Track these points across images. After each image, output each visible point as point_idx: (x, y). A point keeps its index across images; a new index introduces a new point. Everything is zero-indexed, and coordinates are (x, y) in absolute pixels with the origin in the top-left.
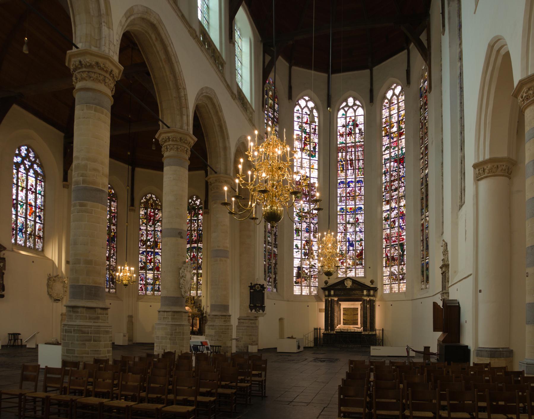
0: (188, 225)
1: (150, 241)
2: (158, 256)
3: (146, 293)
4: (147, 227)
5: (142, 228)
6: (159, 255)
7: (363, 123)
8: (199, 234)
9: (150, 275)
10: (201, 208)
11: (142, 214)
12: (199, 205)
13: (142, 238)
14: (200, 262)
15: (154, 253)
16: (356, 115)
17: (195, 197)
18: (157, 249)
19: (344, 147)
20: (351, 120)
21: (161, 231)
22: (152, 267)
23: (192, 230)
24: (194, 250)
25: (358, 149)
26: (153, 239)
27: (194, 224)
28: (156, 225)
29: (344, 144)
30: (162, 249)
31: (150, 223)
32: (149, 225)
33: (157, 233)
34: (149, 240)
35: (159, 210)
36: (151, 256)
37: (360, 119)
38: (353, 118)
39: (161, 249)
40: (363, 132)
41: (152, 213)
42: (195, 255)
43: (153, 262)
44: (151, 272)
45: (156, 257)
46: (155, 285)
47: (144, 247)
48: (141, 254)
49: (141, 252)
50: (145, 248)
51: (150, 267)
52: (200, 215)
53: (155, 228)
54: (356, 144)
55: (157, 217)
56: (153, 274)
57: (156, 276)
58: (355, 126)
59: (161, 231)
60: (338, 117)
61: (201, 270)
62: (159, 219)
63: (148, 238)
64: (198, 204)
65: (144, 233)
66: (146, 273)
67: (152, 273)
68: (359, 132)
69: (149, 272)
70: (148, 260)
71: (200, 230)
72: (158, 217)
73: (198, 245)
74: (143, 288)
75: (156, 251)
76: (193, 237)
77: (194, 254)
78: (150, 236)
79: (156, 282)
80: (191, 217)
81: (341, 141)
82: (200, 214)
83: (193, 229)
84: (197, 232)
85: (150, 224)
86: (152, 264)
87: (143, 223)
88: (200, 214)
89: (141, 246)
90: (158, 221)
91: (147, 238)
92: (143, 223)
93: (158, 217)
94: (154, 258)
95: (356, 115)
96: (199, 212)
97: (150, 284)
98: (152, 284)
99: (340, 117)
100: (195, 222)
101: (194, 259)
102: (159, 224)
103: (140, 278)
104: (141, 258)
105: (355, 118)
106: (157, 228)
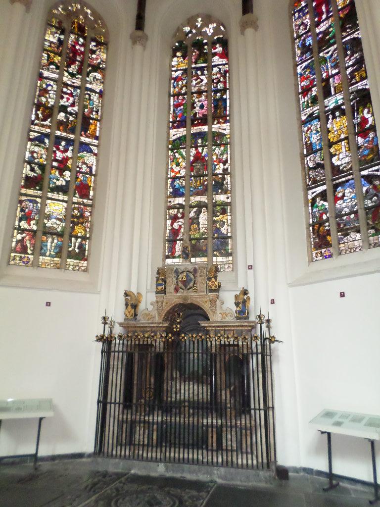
0: (180, 83)
1: (66, 112)
2: (88, 155)
3: (36, 260)
4: (61, 75)
5: (46, 74)
6: (91, 151)
8: (216, 101)
9: (56, 207)
10: (219, 41)
11: (51, 42)
12: (213, 35)
13: (43, 99)
14: (217, 172)
15: (77, 144)
17: (200, 20)
18: (87, 137)
21: (101, 94)
22: (67, 182)
23: (193, 93)
24: (200, 141)
26: (76, 108)
27: (198, 78)
28: (88, 76)
30: (102, 139)
31: (73, 66)
32: (67, 71)
33: (90, 95)
34: (63, 109)
35: (99, 44)
36: (66, 151)
39: (97, 138)
41: (81, 46)
42: (203, 154)
43: (70, 171)
44: (61, 197)
45: (82, 157)
46: (71, 236)
47: (47, 123)
48: (31, 140)
49: (33, 135)
50: (49, 127)
51: (58, 183)
52: (217, 57)
53: (84, 81)
55: (92, 59)
56: (65, 205)
57: (76, 212)
59: (101, 94)
61: (221, 193)
62: (99, 64)
63: (63, 102)
64: (210, 34)
65: (49, 88)
66: (44, 198)
67: (63, 201)
69: (55, 196)
70: (56, 160)
71: (217, 91)
72: (97, 59)
73: (210, 128)
74: (28, 245)
75: (84, 139)
76: (197, 110)
77: (198, 153)
78: (68, 99)
79: (73, 228)
80: (190, 63)
82: (215, 54)
83: (194, 89)
84: (207, 97)
85: (70, 70)
86: (67, 173)
87: (53, 63)
88: (215, 54)
89: (37, 117)
90: (96, 68)
91: (57, 102)
92: (53, 63)
93: (97, 59)
94: (75, 158)
96: (213, 51)
97: (52, 234)
98: (60, 235)
100: (203, 74)
101: (198, 165)
102: (99, 76)
103: (22, 210)
104: (32, 152)
106: (91, 83)
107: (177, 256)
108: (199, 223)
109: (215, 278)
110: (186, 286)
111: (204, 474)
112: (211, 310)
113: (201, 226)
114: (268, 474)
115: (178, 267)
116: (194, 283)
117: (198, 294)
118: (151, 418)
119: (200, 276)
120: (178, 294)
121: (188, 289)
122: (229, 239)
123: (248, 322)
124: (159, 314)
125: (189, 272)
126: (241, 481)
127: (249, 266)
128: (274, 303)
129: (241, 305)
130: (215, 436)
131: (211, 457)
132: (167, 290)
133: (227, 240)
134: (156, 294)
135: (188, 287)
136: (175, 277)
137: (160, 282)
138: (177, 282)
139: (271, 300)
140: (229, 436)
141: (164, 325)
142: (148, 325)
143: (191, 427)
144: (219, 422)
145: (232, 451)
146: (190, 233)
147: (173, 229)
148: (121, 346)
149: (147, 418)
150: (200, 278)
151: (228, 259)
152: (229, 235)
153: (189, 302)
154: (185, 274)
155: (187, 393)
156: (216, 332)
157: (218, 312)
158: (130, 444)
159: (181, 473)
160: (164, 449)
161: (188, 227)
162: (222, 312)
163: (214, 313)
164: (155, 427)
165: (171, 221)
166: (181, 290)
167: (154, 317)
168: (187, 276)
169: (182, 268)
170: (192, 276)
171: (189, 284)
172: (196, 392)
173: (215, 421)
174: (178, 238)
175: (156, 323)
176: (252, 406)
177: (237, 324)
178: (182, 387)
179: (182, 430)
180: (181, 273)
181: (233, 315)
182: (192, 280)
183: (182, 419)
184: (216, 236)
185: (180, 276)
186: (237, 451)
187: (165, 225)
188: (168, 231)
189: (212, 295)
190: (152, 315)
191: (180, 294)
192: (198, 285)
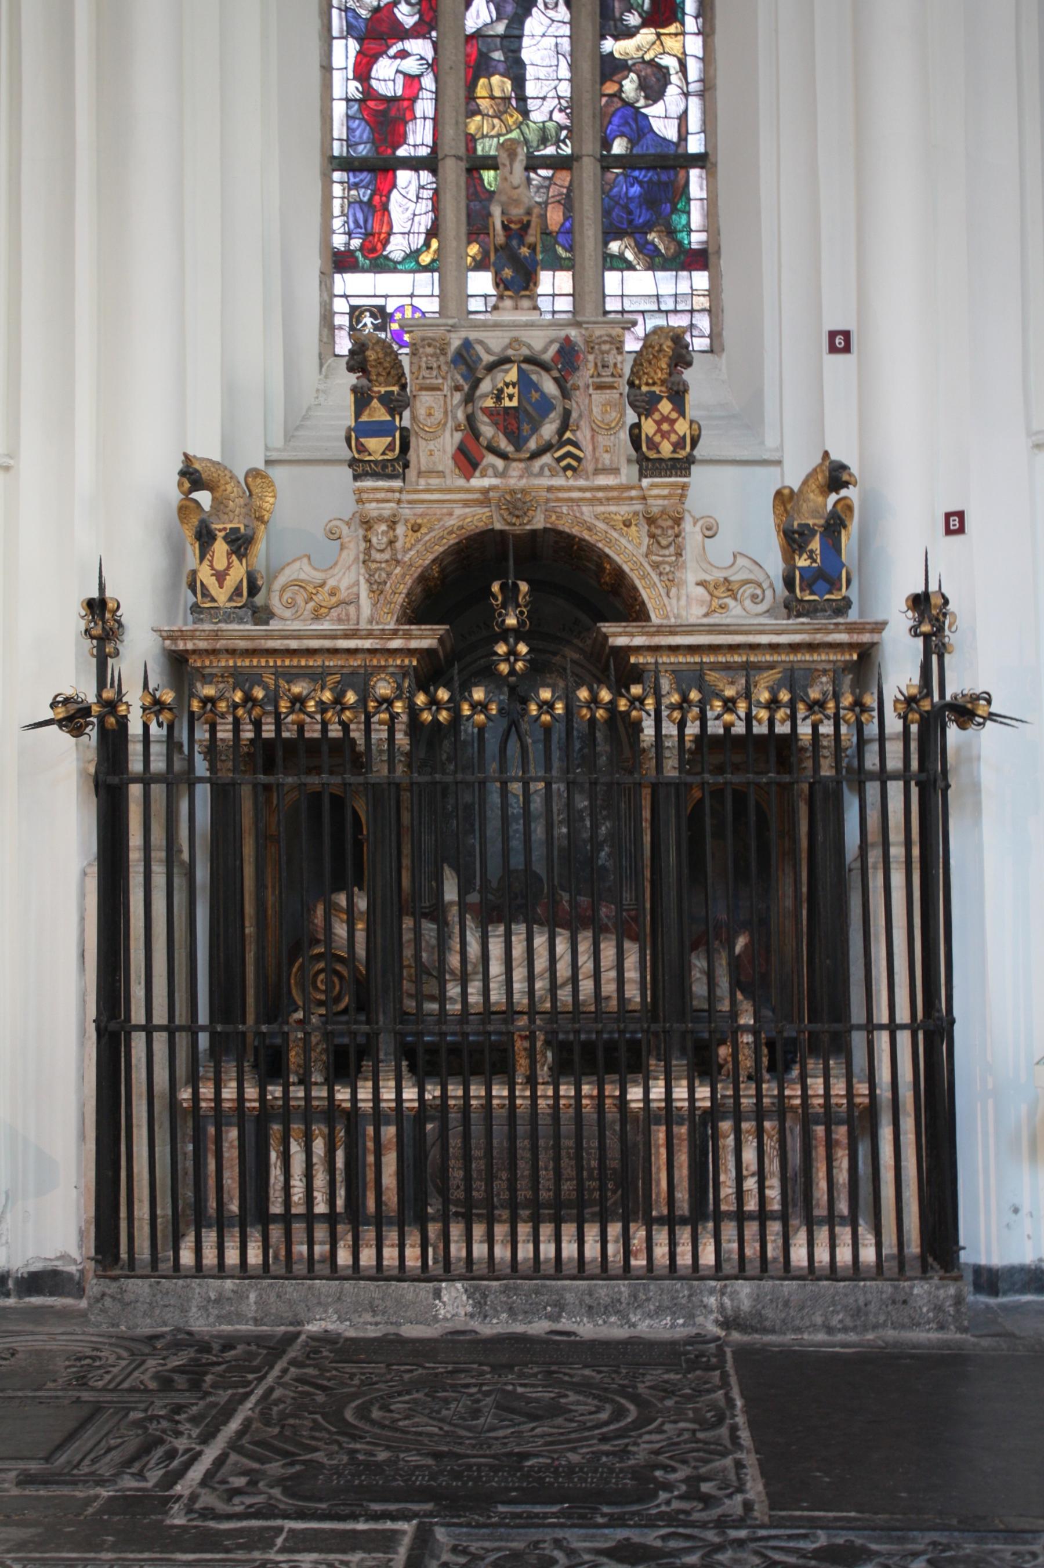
107: (397, 255)
108: (521, 65)
109: (678, 396)
110: (517, 440)
111: (659, 1311)
112: (656, 566)
113: (531, 89)
114: (952, 1291)
115: (473, 335)
116: (564, 426)
117: (581, 482)
118: (365, 1093)
119: (599, 387)
120: (476, 482)
121: (535, 455)
122: (694, 174)
123: (851, 628)
124: (377, 588)
125: (530, 360)
126: (830, 1330)
127: (833, 335)
128: (961, 530)
129: (815, 545)
130: (682, 1158)
131: (666, 1249)
132: (421, 453)
133: (682, 173)
134: (356, 477)
135: (532, 445)
136: (457, 388)
137: (378, 413)
138: (470, 419)
139: (948, 516)
140: (749, 1155)
141: (414, 644)
142: (327, 644)
143: (567, 1127)
144: (703, 1092)
145: (763, 1216)
146: (472, 129)
147: (369, 94)
148: (157, 750)
149: (343, 1094)
150: (598, 397)
151: (684, 288)
152: (695, 145)
153: (539, 522)
154: (513, 375)
155: (519, 974)
156: (684, 679)
157: (691, 575)
158: (265, 1219)
159: (550, 1317)
160: (433, 1230)
161: (462, 94)
162: (708, 578)
163: (671, 582)
164: (389, 1132)
165: (353, 46)
166: (490, 459)
167: (355, 601)
168: (525, 383)
169: (496, 342)
170: (550, 387)
171: (535, 429)
172: (563, 969)
173: (680, 1092)
174: (402, 152)
175: (369, 635)
176: (857, 1015)
177: (797, 638)
178: (496, 948)
179: (523, 1144)
180: (491, 367)
181: (769, 593)
182: (552, 407)
183: (523, 1092)
184: (619, 147)
185: (486, 386)
186: (784, 1217)
187: (327, 68)
188: (339, 109)
189: (657, 486)
190: (332, 594)
191: (486, 482)
192: (583, 436)
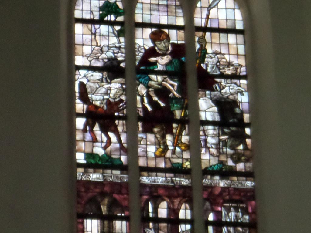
7: (243, 71)
16: (199, 20)
19: (119, 187)
20: (161, 46)
25: (218, 214)
29: (123, 168)
37: (224, 50)
38: (176, 37)
40: (246, 117)
54: (207, 181)
58: (192, 80)
60: (77, 14)
68: (217, 118)
81: (99, 151)
95: (199, 20)
99: (88, 16)
105: (190, 39)
